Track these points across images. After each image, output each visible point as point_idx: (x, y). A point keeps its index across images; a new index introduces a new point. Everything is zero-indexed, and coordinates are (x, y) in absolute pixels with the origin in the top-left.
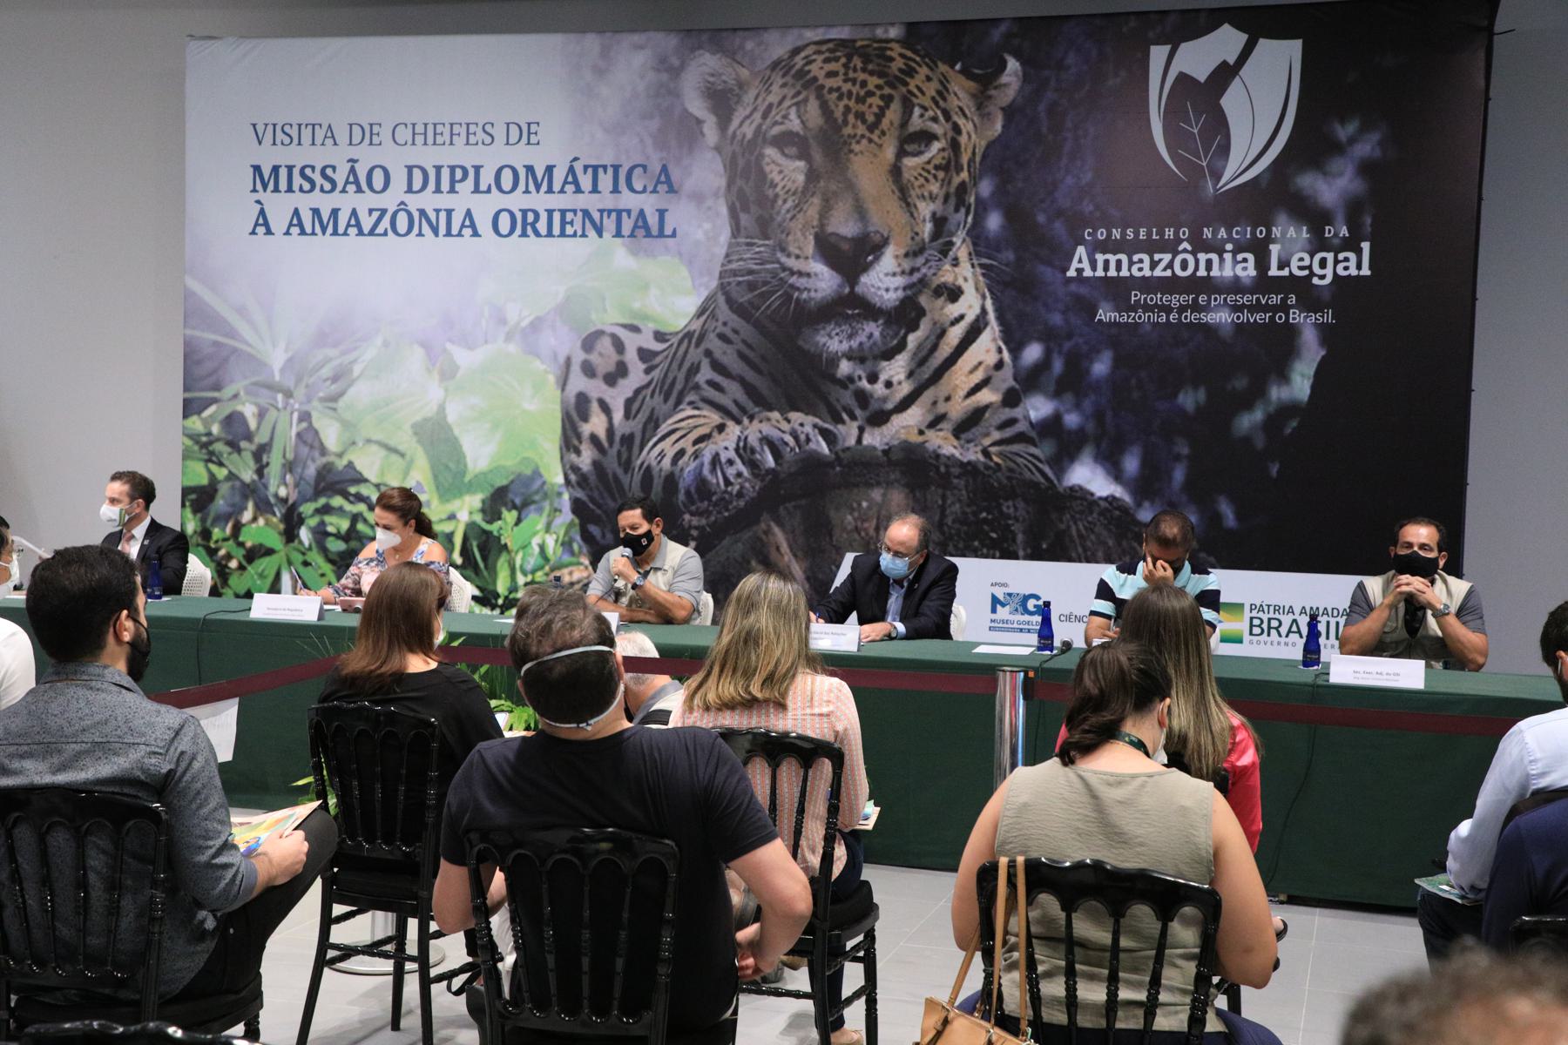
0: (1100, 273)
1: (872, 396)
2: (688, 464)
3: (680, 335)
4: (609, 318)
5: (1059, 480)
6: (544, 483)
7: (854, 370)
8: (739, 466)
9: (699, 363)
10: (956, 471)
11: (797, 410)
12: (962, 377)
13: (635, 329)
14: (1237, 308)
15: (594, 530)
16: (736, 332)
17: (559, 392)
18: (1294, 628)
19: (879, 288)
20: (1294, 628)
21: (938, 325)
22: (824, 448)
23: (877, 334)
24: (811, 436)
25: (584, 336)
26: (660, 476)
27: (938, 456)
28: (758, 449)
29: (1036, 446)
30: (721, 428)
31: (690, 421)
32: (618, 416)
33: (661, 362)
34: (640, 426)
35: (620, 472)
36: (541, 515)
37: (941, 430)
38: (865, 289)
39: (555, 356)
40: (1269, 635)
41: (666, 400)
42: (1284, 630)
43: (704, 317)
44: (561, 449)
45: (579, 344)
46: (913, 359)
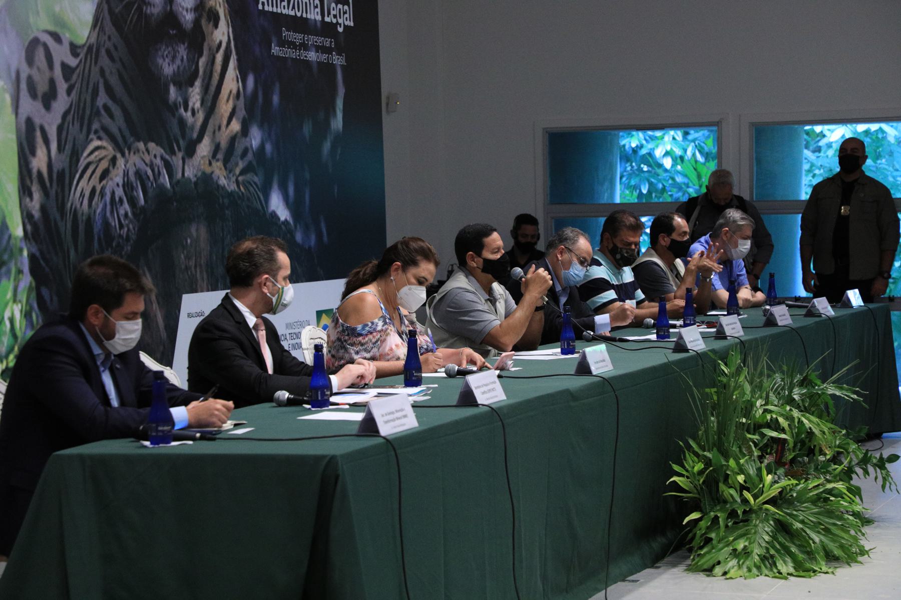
0: (271, 10)
1: (186, 125)
2: (97, 205)
3: (86, 48)
4: (41, 24)
5: (267, 207)
6: (10, 237)
7: (177, 96)
8: (126, 206)
9: (98, 83)
10: (226, 201)
11: (153, 141)
12: (225, 107)
13: (57, 38)
14: (320, 49)
15: (45, 292)
16: (116, 48)
17: (13, 117)
19: (183, 8)
21: (211, 52)
22: (165, 180)
23: (185, 57)
24: (160, 169)
25: (27, 44)
26: (82, 221)
27: (218, 186)
28: (135, 185)
29: (256, 175)
30: (113, 161)
31: (96, 153)
32: (54, 146)
33: (76, 82)
34: (68, 160)
35: (58, 218)
36: (9, 279)
37: (218, 160)
38: (177, 8)
39: (9, 68)
41: (81, 130)
43: (98, 28)
44: (19, 191)
45: (23, 54)
46: (203, 86)
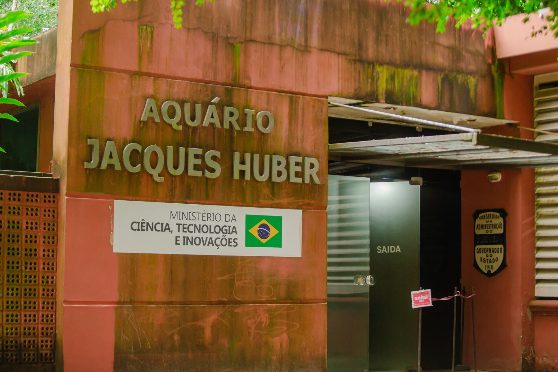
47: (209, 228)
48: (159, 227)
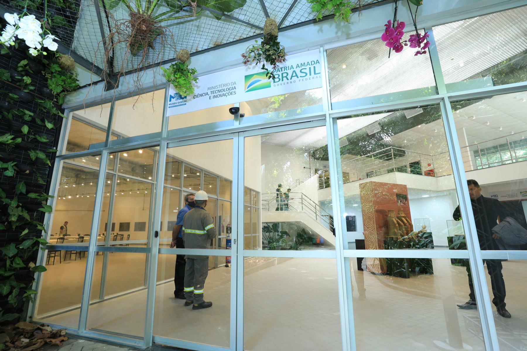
18: (294, 75)
20: (294, 75)
40: (282, 80)
42: (289, 77)
47: (224, 90)
48: (204, 95)
